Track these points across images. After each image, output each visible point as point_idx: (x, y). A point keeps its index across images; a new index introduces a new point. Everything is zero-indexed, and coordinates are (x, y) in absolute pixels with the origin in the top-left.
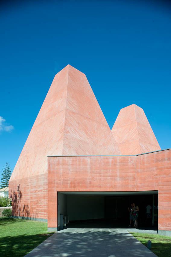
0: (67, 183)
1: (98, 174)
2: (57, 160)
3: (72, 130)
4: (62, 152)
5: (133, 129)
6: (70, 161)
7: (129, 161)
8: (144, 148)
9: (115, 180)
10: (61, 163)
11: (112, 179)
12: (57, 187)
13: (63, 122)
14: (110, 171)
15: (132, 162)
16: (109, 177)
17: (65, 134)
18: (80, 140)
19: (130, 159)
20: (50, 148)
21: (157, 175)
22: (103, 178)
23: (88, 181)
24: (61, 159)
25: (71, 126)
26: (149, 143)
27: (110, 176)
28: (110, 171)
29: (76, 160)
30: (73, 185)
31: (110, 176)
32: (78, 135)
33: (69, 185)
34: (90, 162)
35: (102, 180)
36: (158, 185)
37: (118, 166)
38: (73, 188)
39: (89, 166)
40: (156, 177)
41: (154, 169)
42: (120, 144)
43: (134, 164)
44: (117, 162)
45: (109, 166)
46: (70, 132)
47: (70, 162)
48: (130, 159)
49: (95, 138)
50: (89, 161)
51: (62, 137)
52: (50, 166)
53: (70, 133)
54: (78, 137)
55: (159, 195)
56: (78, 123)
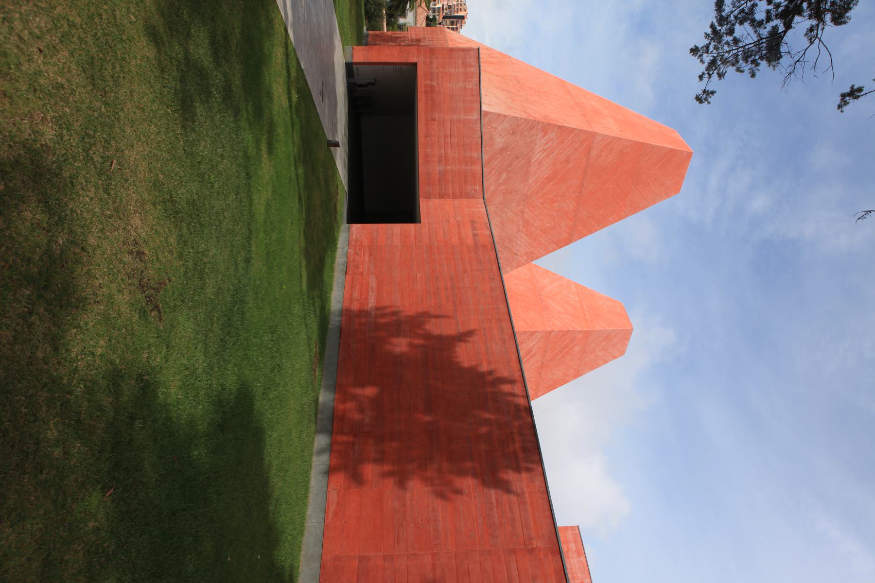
0: (432, 80)
1: (449, 133)
2: (473, 64)
3: (551, 142)
4: (500, 113)
5: (573, 321)
7: (474, 187)
8: (531, 344)
9: (440, 162)
10: (468, 69)
11: (440, 157)
12: (425, 63)
13: (565, 123)
14: (455, 152)
15: (473, 192)
16: (443, 152)
17: (540, 126)
18: (530, 161)
19: (477, 188)
20: (511, 99)
22: (443, 141)
23: (436, 115)
24: (474, 70)
25: (558, 141)
26: (543, 363)
28: (455, 152)
29: (473, 96)
30: (429, 89)
32: (543, 156)
33: (429, 82)
34: (470, 120)
35: (438, 140)
36: (429, 224)
37: (463, 167)
38: (423, 89)
39: (462, 117)
40: (445, 221)
41: (459, 219)
42: (539, 294)
43: (469, 195)
44: (471, 166)
45: (464, 151)
46: (546, 137)
47: (469, 86)
49: (540, 201)
50: (471, 118)
51: (534, 118)
52: (462, 52)
53: (544, 136)
54: (537, 156)
56: (567, 161)
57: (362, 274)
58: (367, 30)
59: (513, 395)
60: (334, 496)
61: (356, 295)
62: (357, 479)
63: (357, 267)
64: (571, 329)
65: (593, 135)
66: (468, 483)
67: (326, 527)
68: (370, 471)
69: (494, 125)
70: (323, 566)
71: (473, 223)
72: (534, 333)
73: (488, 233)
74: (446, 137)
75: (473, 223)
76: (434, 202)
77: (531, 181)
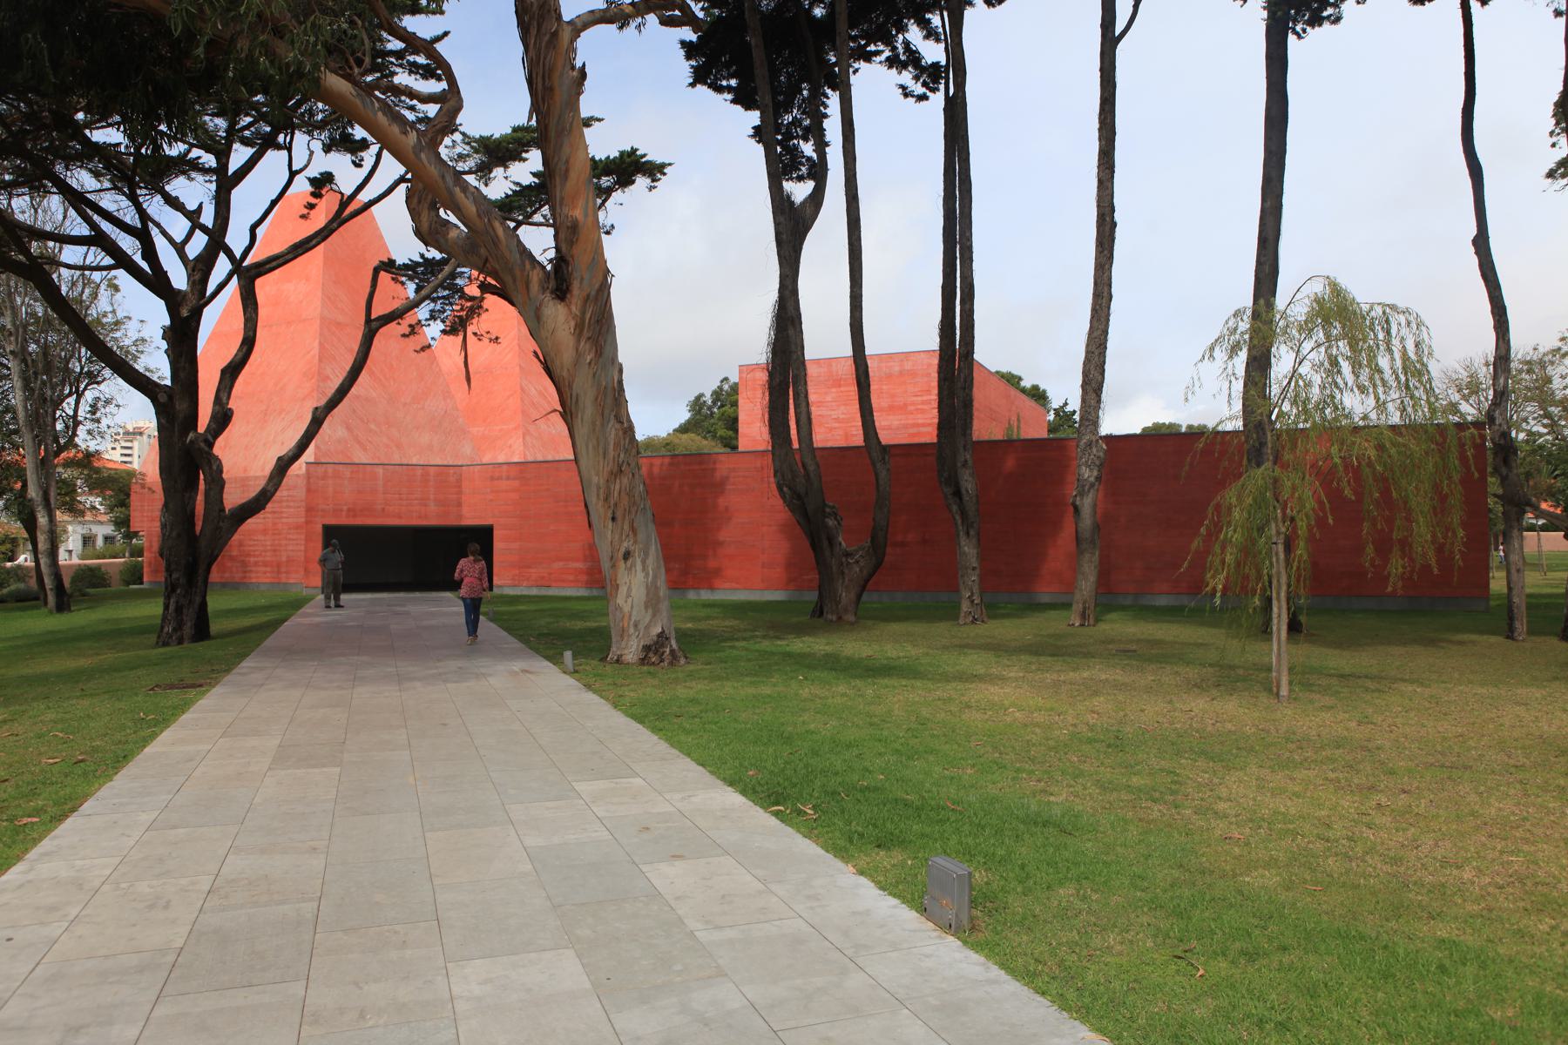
0: (342, 510)
1: (397, 496)
6: (347, 472)
8: (533, 392)
9: (426, 505)
17: (321, 384)
19: (452, 471)
21: (491, 500)
24: (330, 469)
27: (416, 499)
31: (416, 499)
39: (381, 483)
41: (488, 490)
47: (348, 474)
48: (452, 471)
53: (331, 380)
55: (495, 532)
57: (550, 574)
58: (142, 583)
59: (662, 465)
60: (727, 585)
61: (571, 578)
62: (717, 572)
63: (543, 578)
64: (516, 341)
65: (323, 319)
66: (722, 502)
67: (745, 589)
68: (712, 563)
69: (327, 438)
71: (492, 478)
72: (522, 389)
73: (505, 467)
74: (401, 499)
75: (492, 478)
76: (465, 511)
77: (374, 394)
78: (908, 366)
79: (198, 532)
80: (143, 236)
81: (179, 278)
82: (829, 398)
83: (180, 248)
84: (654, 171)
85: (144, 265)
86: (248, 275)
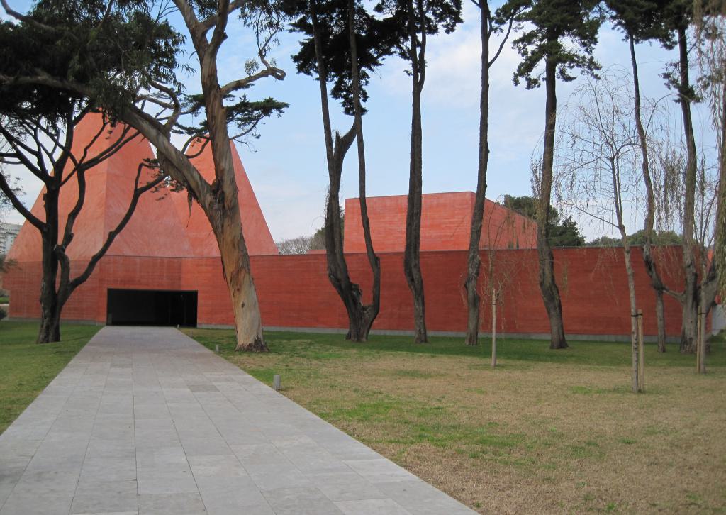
0: (117, 281)
48: (176, 260)
65: (108, 174)
70: (341, 328)
75: (198, 265)
78: (442, 201)
79: (57, 291)
80: (38, 154)
81: (50, 168)
82: (396, 219)
83: (50, 156)
84: (279, 107)
85: (39, 168)
86: (81, 169)
